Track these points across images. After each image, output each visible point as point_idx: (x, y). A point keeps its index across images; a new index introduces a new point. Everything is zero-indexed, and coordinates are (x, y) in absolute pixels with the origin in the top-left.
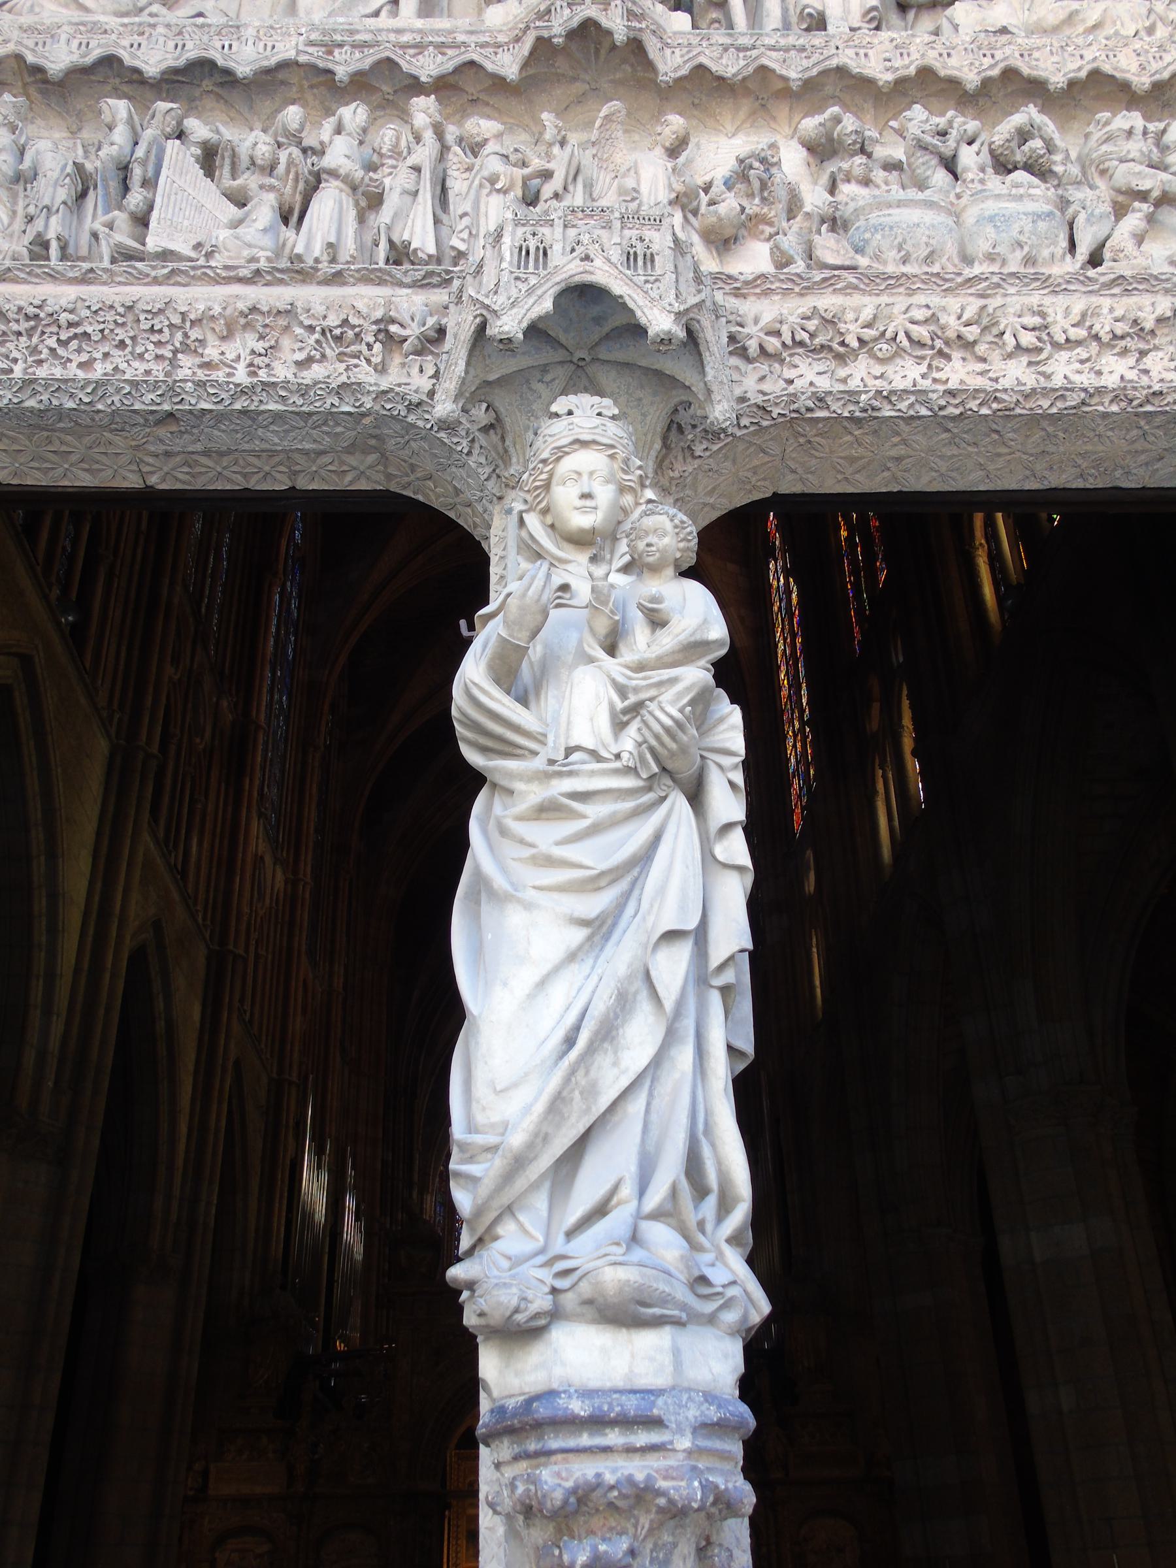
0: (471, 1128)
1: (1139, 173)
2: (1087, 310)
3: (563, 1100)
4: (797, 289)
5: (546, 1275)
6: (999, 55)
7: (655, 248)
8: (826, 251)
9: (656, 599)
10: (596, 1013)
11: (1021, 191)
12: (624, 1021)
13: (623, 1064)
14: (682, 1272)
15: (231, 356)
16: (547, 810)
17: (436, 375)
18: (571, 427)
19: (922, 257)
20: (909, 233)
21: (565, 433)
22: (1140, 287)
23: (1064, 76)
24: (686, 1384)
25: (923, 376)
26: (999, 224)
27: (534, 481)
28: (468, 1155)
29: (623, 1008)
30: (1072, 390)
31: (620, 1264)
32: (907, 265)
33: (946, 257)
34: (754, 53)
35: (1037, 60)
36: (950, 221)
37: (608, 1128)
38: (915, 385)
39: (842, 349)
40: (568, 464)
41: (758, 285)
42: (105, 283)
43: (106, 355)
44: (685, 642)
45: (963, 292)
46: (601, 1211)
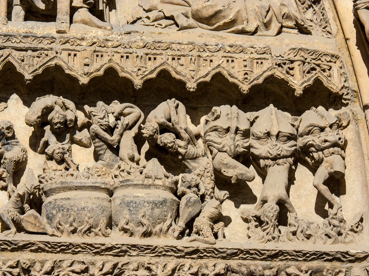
1: (226, 164)
2: (177, 267)
4: (9, 248)
6: (159, 61)
8: (28, 224)
11: (150, 181)
19: (83, 230)
20: (77, 214)
22: (208, 255)
23: (195, 81)
26: (132, 209)
32: (76, 234)
33: (99, 228)
34: (6, 52)
35: (182, 65)
45: (105, 253)
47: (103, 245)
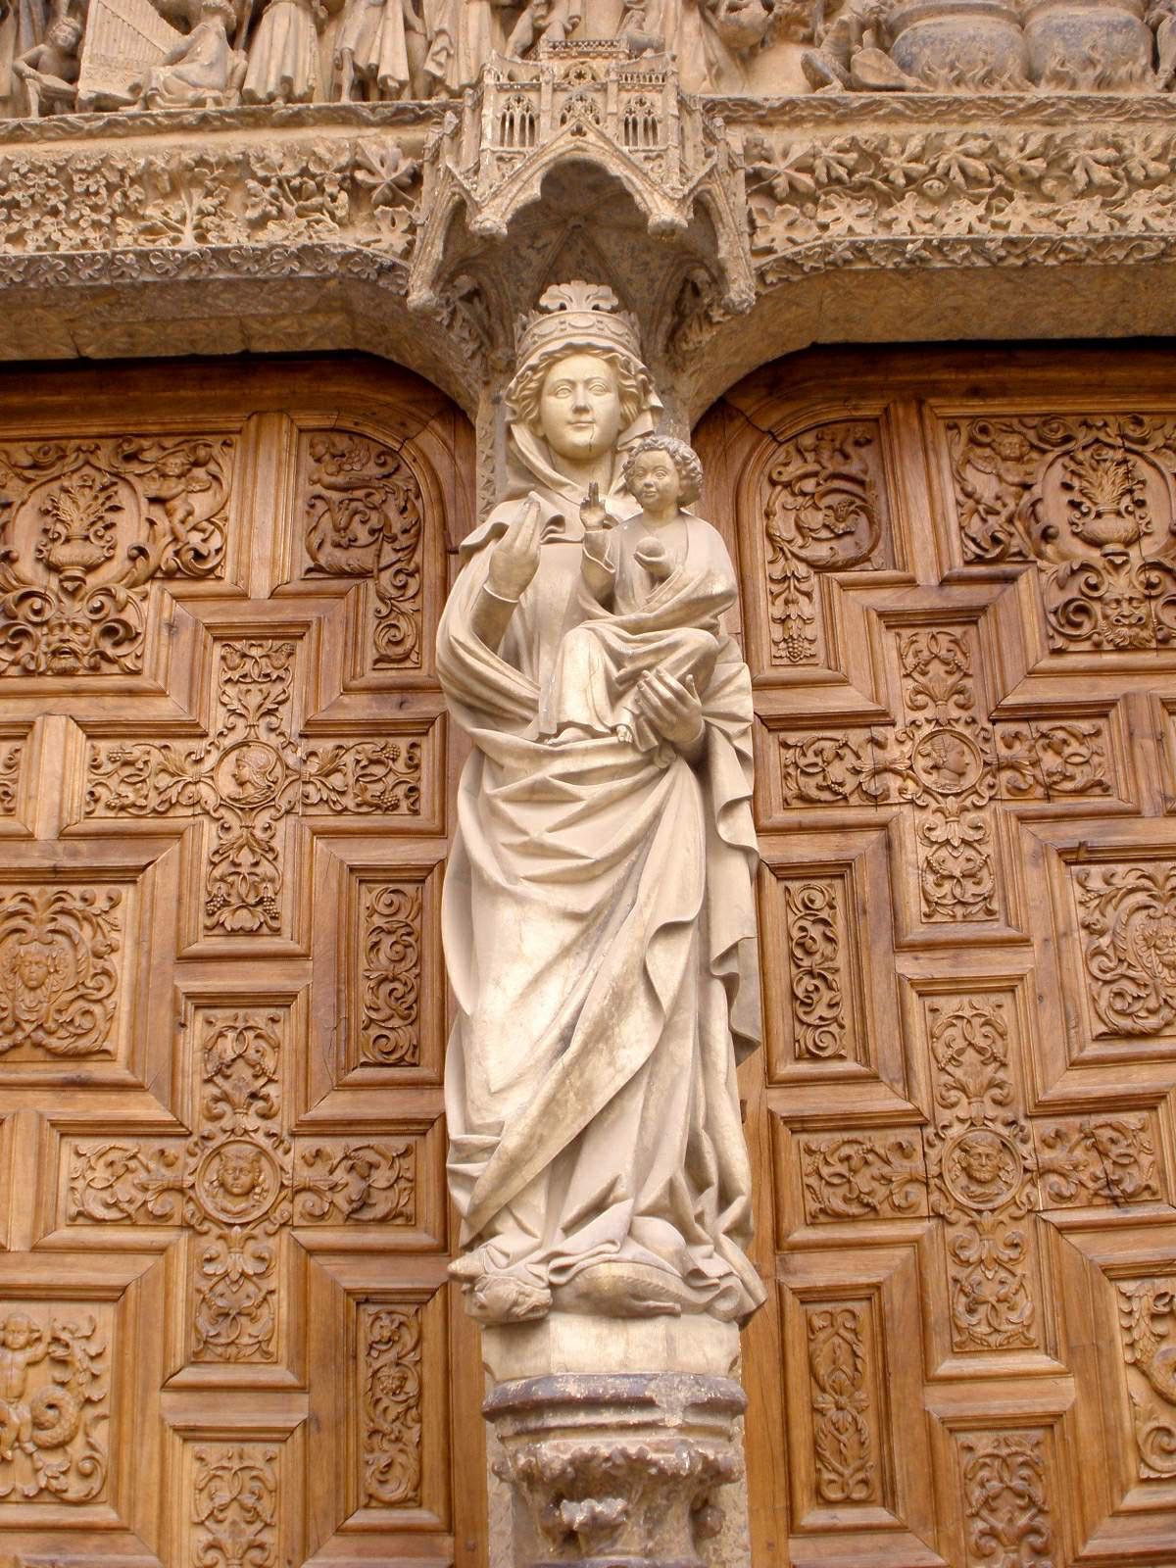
0: (470, 1128)
3: (558, 1103)
4: (832, 116)
5: (543, 1270)
7: (658, 113)
9: (652, 552)
12: (620, 1020)
13: (619, 1063)
15: (175, 215)
16: (540, 795)
17: (412, 229)
21: (556, 334)
24: (678, 1368)
25: (981, 219)
30: (1150, 239)
36: (1013, 30)
38: (970, 231)
39: (884, 187)
40: (564, 371)
41: (787, 113)
42: (33, 141)
43: (37, 225)
47: (1021, 99)
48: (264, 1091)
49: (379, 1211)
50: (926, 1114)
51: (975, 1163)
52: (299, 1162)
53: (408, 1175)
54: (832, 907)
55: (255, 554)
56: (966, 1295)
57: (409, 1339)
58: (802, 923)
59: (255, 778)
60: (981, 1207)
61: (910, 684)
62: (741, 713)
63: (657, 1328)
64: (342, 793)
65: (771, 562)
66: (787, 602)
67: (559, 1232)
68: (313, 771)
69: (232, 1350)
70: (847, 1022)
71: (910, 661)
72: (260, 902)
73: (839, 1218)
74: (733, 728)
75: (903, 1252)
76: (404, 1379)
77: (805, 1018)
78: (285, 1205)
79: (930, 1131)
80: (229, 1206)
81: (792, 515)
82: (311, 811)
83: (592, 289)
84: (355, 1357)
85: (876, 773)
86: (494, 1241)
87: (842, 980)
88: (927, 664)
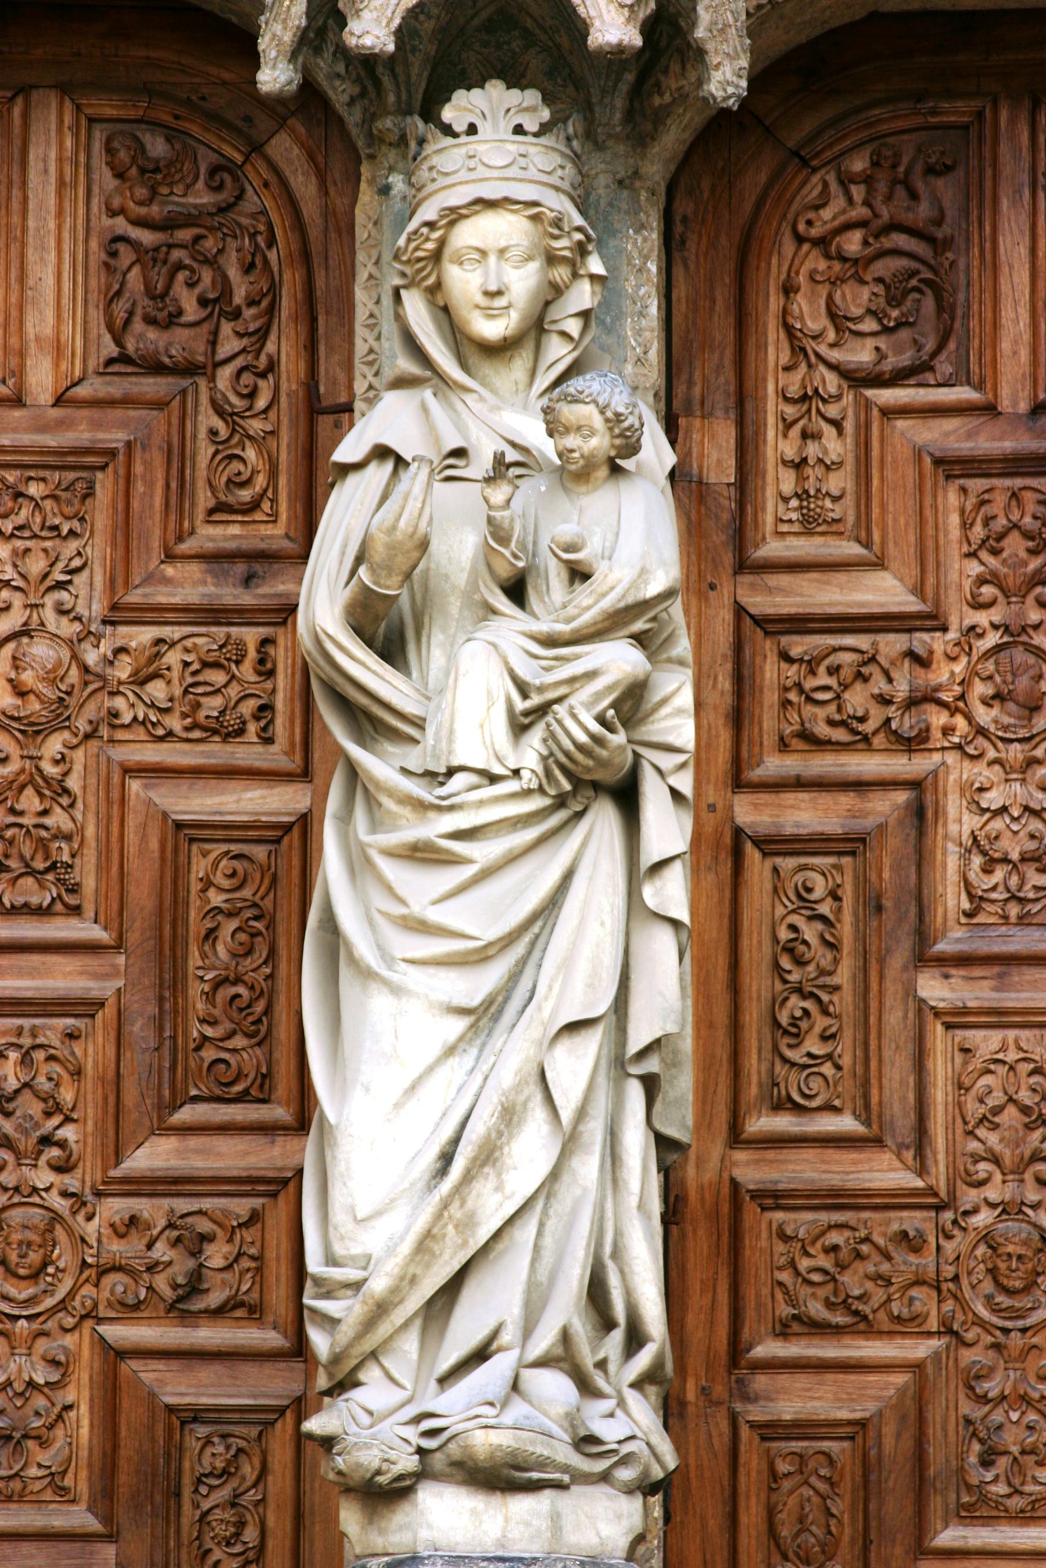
0: (332, 1260)
3: (434, 1237)
5: (411, 1433)
10: (474, 1137)
12: (511, 1136)
13: (508, 1191)
14: (566, 1431)
18: (472, 164)
21: (463, 175)
24: (566, 1550)
27: (417, 249)
28: (324, 1290)
29: (509, 1123)
31: (492, 1427)
37: (491, 1257)
44: (611, 610)
46: (481, 1355)
48: (61, 1133)
49: (215, 1299)
50: (943, 1194)
51: (1002, 1266)
52: (106, 1231)
53: (253, 1251)
54: (837, 898)
55: (30, 331)
56: (982, 1441)
57: (249, 1470)
58: (794, 919)
59: (42, 688)
60: (1009, 1324)
61: (974, 568)
62: (678, 743)
63: (543, 1501)
64: (167, 711)
65: (787, 369)
66: (805, 435)
67: (433, 1385)
68: (124, 675)
69: (16, 1485)
70: (846, 1061)
71: (978, 531)
72: (53, 867)
73: (818, 1328)
74: (667, 761)
75: (900, 1379)
76: (241, 1524)
77: (789, 1054)
78: (87, 1290)
79: (948, 1216)
80: (12, 1291)
81: (823, 291)
82: (120, 735)
83: (514, 96)
84: (178, 1495)
85: (913, 702)
86: (356, 1394)
87: (844, 1002)
88: (1001, 537)
